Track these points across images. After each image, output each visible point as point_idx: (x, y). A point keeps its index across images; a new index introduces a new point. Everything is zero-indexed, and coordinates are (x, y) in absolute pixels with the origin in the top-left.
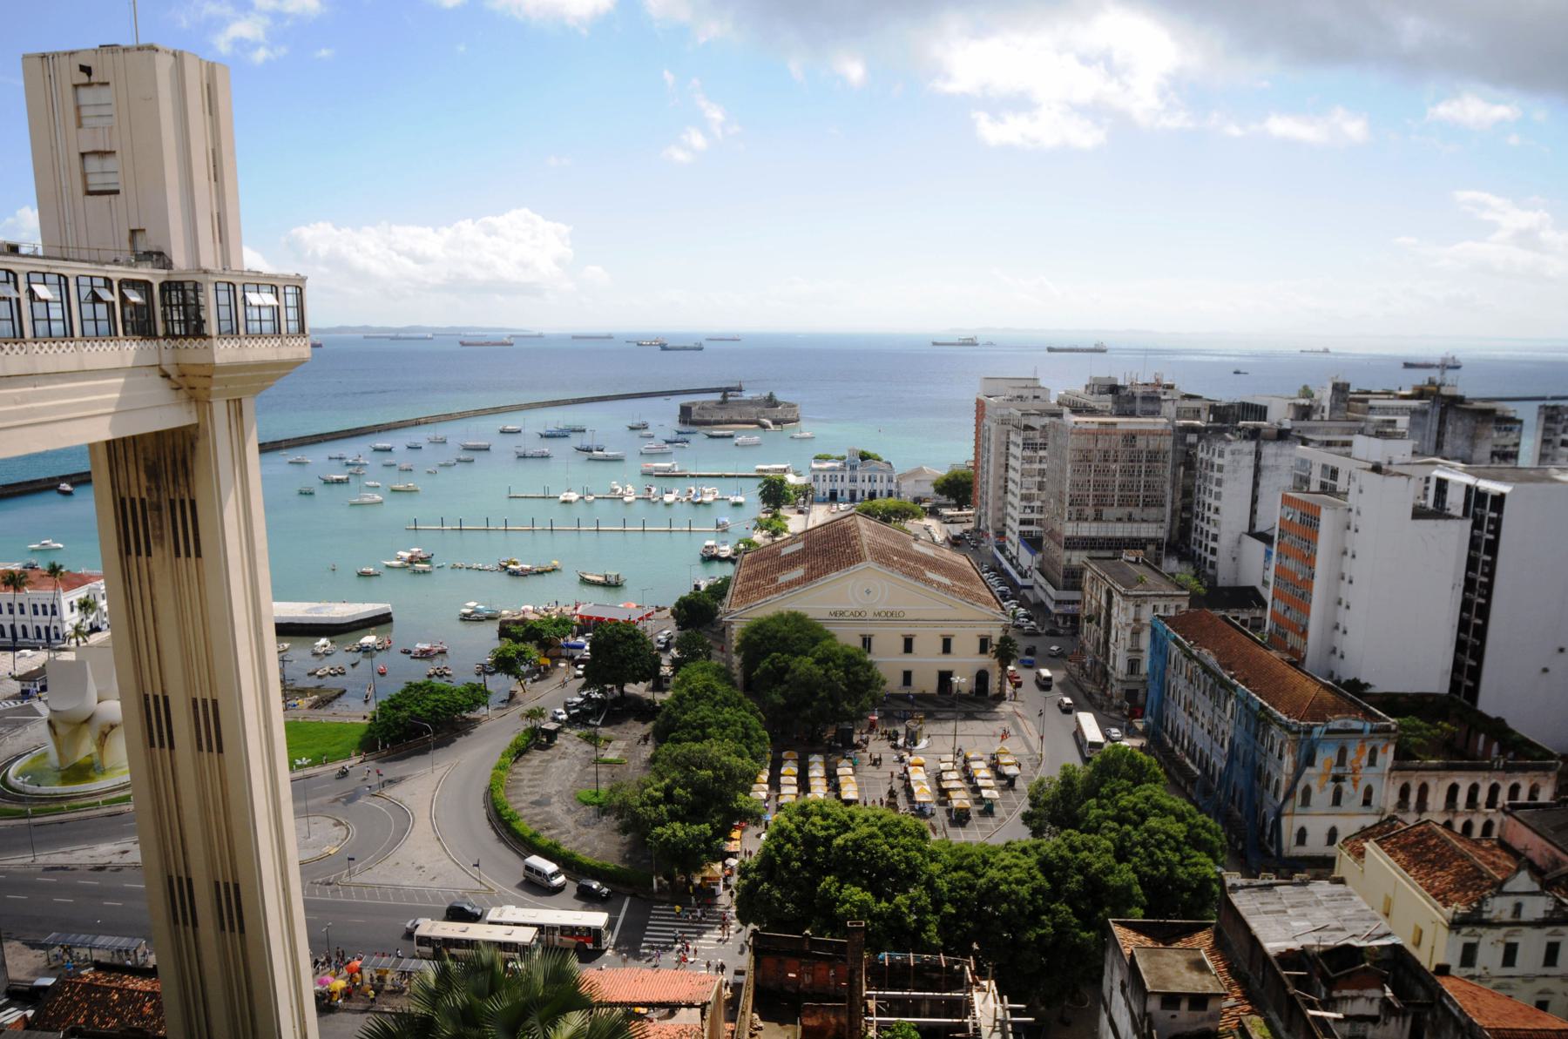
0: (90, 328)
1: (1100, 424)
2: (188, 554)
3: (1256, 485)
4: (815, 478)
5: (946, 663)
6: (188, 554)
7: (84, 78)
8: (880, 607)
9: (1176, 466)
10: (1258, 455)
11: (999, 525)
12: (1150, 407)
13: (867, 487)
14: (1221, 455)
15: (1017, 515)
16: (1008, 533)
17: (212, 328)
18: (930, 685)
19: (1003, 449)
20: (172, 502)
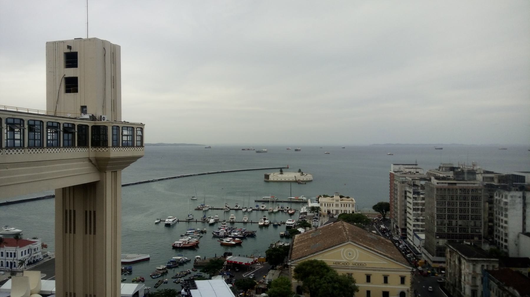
0: (66, 142)
1: (449, 184)
2: (90, 233)
3: (524, 211)
4: (321, 205)
6: (90, 233)
8: (355, 261)
9: (485, 202)
10: (524, 198)
11: (403, 227)
12: (471, 177)
13: (343, 209)
14: (506, 198)
15: (412, 223)
16: (408, 230)
17: (110, 143)
19: (403, 194)
20: (86, 212)
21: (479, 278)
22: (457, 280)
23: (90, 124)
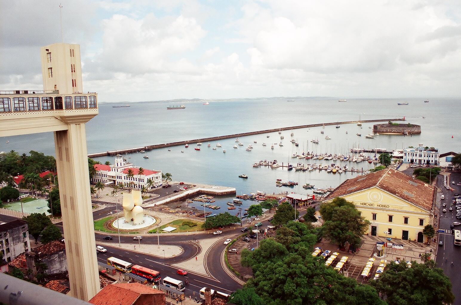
5: (406, 227)
7: (47, 52)
13: (426, 159)
18: (400, 236)
23: (54, 96)
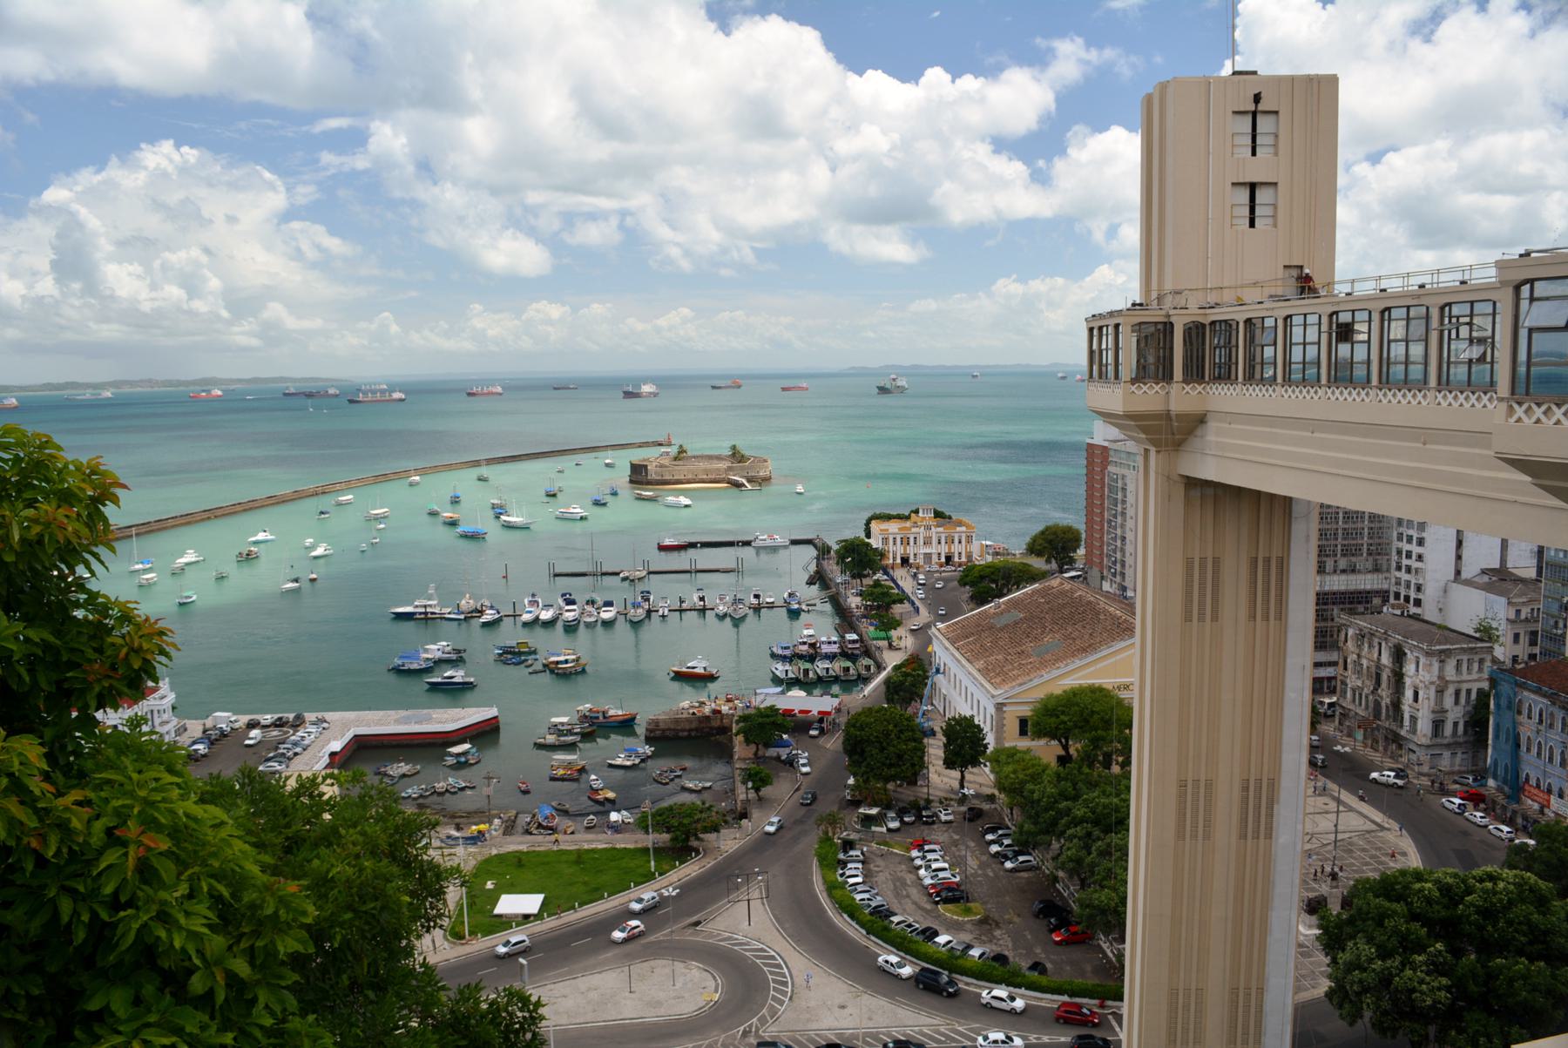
4: (885, 540)
13: (944, 549)
21: (1451, 690)
22: (1386, 701)
